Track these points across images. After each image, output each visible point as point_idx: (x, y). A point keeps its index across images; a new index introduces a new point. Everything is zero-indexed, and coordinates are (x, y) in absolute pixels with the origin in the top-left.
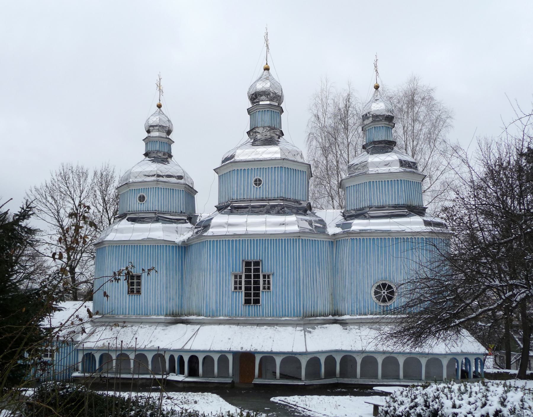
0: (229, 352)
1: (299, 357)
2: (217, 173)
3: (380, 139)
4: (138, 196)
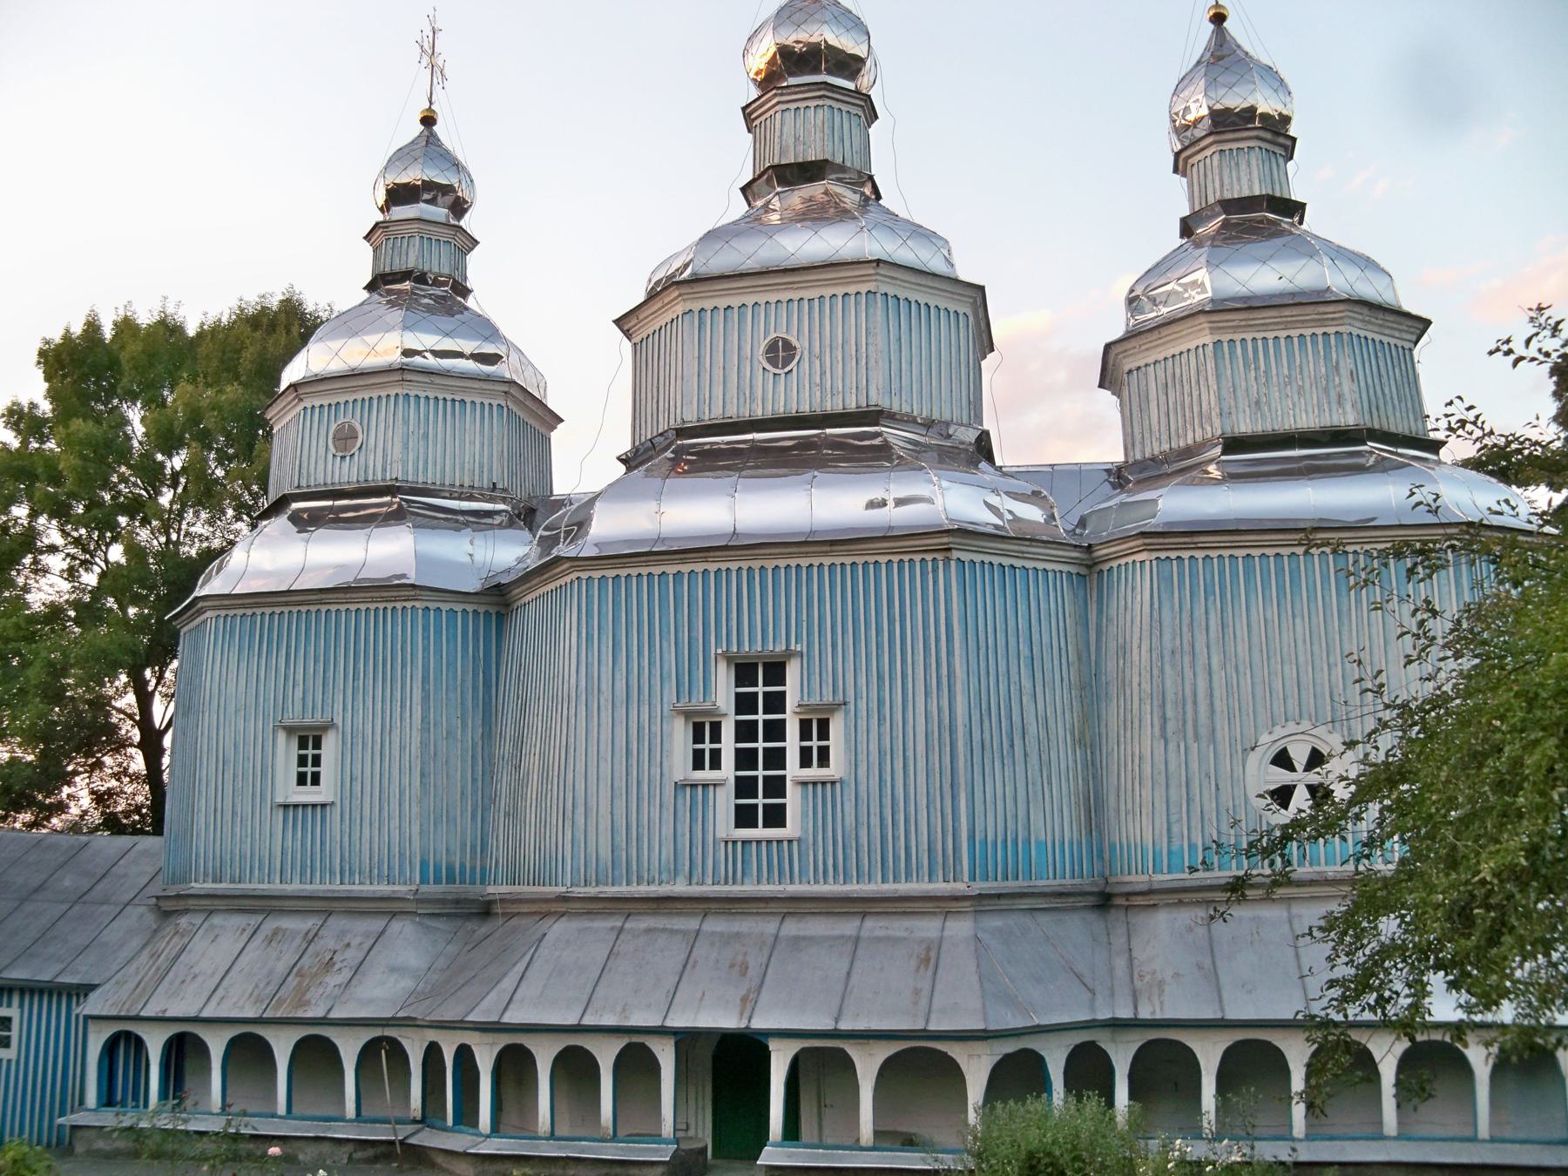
0: (661, 1031)
1: (955, 1051)
2: (628, 334)
3: (1246, 193)
4: (333, 427)
